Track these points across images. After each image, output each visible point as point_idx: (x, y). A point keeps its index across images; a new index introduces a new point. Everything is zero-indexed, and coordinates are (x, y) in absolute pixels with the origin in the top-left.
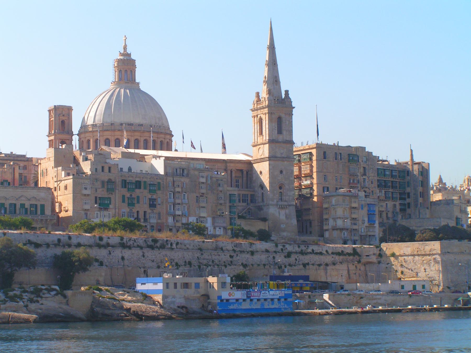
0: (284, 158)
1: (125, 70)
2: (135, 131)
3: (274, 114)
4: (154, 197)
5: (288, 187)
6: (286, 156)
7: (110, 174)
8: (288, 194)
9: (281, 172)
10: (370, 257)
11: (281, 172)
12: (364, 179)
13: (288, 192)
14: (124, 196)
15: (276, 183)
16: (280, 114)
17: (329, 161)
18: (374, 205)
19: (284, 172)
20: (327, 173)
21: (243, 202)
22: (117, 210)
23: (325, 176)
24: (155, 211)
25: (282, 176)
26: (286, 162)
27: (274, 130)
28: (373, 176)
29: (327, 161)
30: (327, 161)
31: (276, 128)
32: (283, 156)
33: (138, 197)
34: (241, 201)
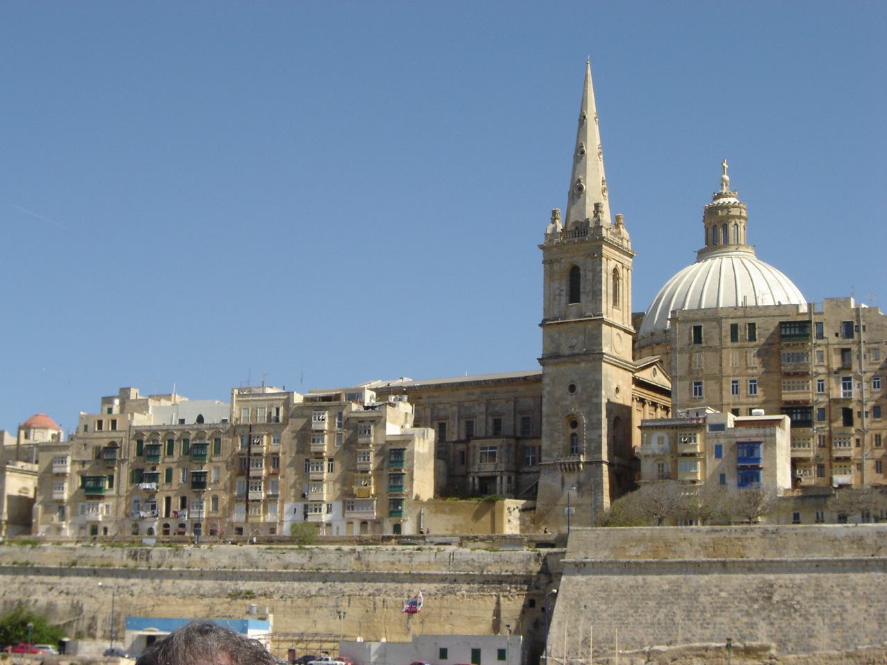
9: (572, 388)
11: (572, 388)
12: (845, 379)
16: (575, 259)
19: (579, 389)
25: (574, 396)
26: (583, 365)
27: (557, 298)
32: (576, 351)
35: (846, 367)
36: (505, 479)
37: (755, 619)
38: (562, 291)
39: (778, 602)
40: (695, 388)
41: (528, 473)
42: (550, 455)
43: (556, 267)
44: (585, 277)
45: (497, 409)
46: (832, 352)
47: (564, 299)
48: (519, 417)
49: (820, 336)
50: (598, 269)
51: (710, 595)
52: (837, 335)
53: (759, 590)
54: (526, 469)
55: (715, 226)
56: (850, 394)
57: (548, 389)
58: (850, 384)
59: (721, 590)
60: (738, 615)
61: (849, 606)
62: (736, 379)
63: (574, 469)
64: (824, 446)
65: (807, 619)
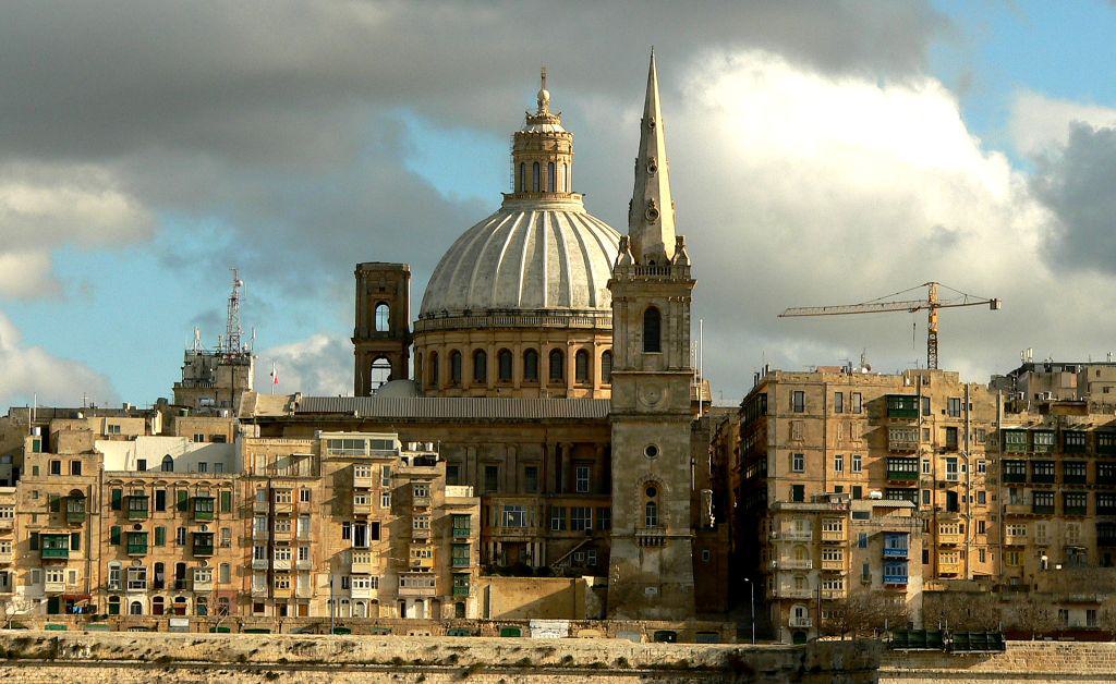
0: (659, 414)
1: (533, 161)
2: (521, 329)
3: (635, 301)
4: (210, 528)
6: (666, 410)
7: (78, 479)
10: (777, 677)
11: (652, 451)
12: (948, 459)
13: (670, 503)
17: (814, 417)
18: (906, 533)
20: (805, 452)
21: (574, 528)
22: (95, 565)
24: (209, 563)
26: (666, 424)
27: (632, 343)
29: (806, 417)
30: (806, 417)
31: (641, 338)
32: (658, 408)
34: (569, 527)
35: (952, 447)
36: (537, 546)
38: (638, 335)
40: (796, 461)
41: (558, 539)
42: (624, 527)
43: (630, 306)
44: (669, 322)
45: (491, 455)
46: (937, 428)
47: (640, 346)
48: (522, 467)
49: (927, 412)
50: (685, 315)
52: (943, 412)
54: (555, 535)
55: (536, 163)
56: (955, 477)
58: (955, 466)
62: (839, 453)
63: (657, 542)
64: (928, 531)
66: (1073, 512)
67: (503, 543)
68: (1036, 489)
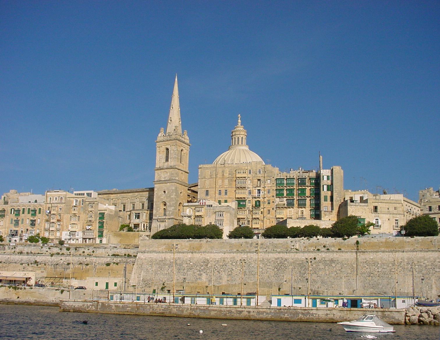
4: (35, 218)
5: (169, 204)
8: (169, 210)
9: (165, 192)
11: (165, 192)
12: (258, 190)
13: (169, 208)
14: (12, 219)
15: (159, 202)
16: (166, 146)
17: (212, 178)
19: (166, 192)
20: (209, 189)
23: (206, 191)
28: (271, 187)
32: (166, 179)
33: (23, 220)
37: (202, 273)
39: (210, 266)
42: (156, 216)
45: (143, 200)
51: (187, 264)
53: (204, 262)
56: (260, 195)
57: (156, 192)
59: (191, 262)
60: (196, 271)
61: (234, 269)
62: (220, 189)
65: (219, 273)
66: (302, 205)
67: (134, 224)
68: (288, 198)
